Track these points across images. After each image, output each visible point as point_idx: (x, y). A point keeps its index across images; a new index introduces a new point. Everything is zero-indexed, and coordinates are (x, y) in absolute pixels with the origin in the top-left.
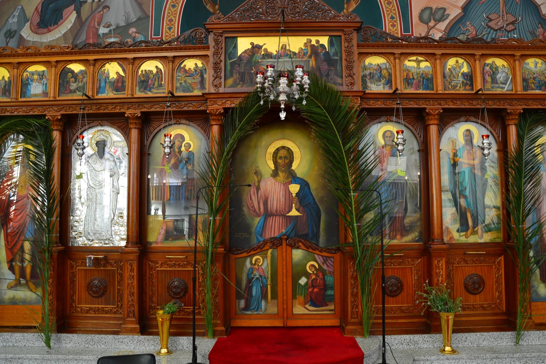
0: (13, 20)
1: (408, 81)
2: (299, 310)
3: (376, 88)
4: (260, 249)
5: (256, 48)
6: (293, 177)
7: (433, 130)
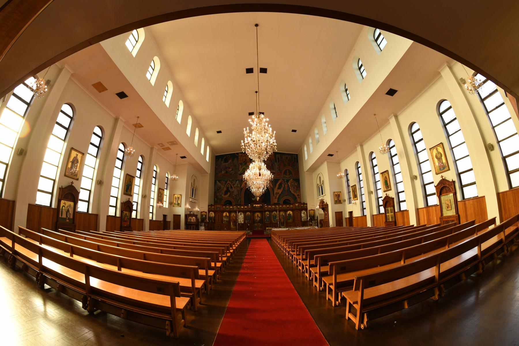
0: (221, 194)
1: (269, 208)
2: (259, 229)
3: (266, 209)
4: (256, 223)
5: (255, 206)
6: (259, 217)
7: (271, 213)
